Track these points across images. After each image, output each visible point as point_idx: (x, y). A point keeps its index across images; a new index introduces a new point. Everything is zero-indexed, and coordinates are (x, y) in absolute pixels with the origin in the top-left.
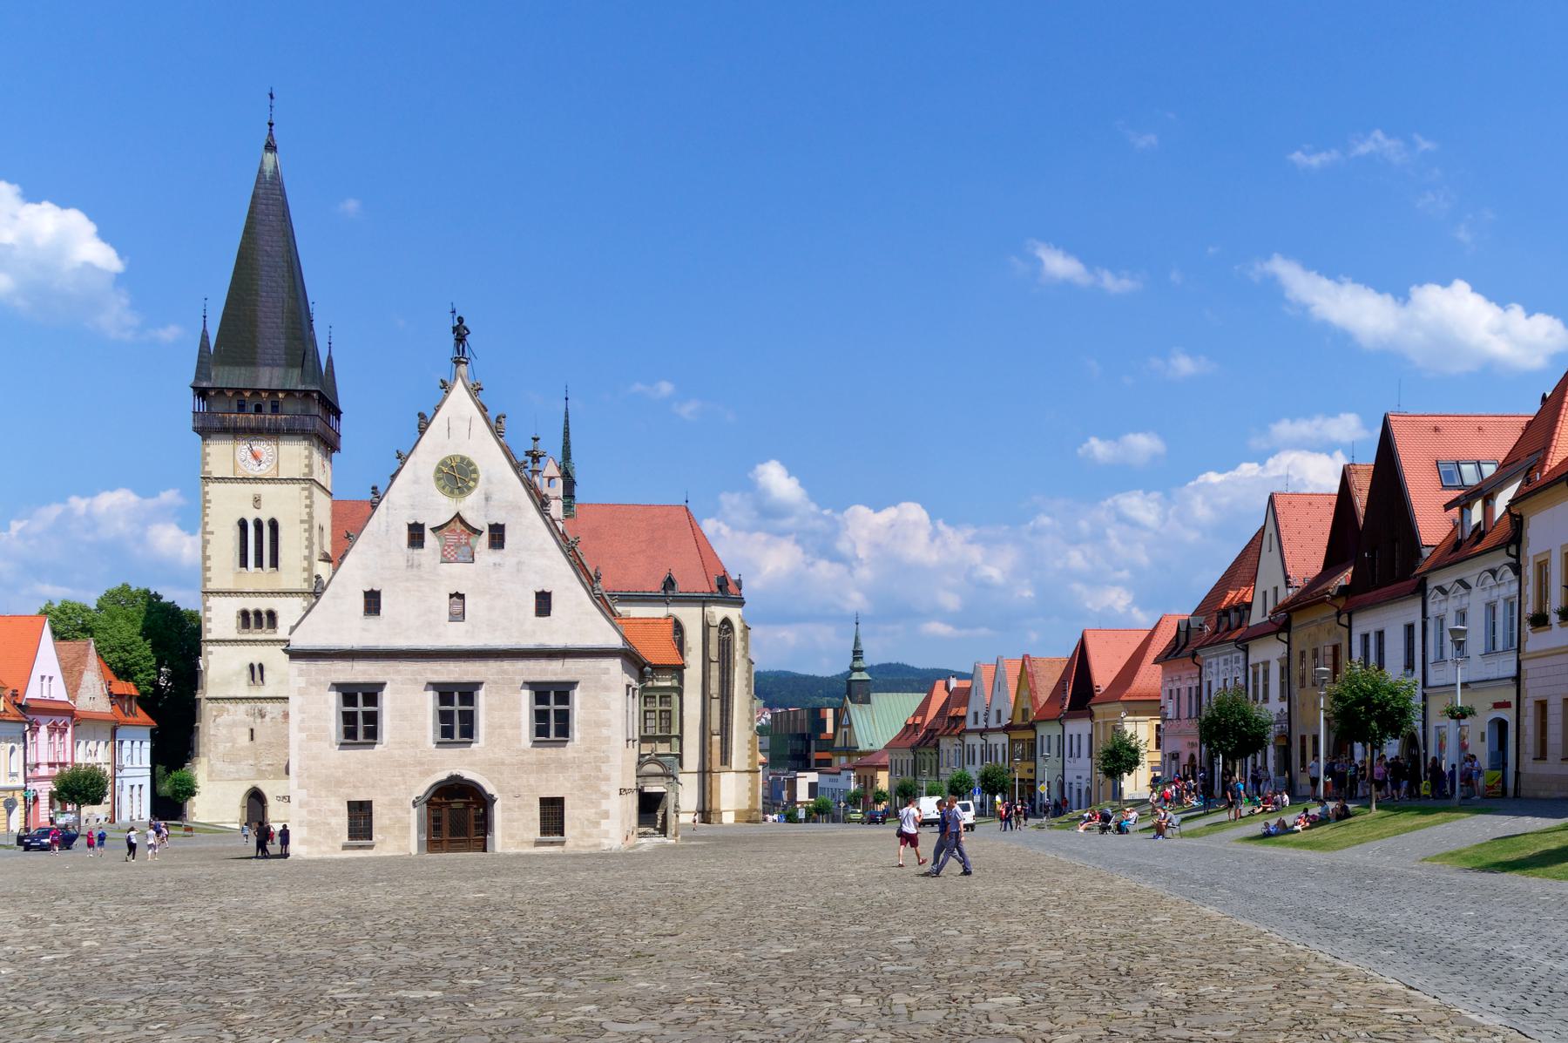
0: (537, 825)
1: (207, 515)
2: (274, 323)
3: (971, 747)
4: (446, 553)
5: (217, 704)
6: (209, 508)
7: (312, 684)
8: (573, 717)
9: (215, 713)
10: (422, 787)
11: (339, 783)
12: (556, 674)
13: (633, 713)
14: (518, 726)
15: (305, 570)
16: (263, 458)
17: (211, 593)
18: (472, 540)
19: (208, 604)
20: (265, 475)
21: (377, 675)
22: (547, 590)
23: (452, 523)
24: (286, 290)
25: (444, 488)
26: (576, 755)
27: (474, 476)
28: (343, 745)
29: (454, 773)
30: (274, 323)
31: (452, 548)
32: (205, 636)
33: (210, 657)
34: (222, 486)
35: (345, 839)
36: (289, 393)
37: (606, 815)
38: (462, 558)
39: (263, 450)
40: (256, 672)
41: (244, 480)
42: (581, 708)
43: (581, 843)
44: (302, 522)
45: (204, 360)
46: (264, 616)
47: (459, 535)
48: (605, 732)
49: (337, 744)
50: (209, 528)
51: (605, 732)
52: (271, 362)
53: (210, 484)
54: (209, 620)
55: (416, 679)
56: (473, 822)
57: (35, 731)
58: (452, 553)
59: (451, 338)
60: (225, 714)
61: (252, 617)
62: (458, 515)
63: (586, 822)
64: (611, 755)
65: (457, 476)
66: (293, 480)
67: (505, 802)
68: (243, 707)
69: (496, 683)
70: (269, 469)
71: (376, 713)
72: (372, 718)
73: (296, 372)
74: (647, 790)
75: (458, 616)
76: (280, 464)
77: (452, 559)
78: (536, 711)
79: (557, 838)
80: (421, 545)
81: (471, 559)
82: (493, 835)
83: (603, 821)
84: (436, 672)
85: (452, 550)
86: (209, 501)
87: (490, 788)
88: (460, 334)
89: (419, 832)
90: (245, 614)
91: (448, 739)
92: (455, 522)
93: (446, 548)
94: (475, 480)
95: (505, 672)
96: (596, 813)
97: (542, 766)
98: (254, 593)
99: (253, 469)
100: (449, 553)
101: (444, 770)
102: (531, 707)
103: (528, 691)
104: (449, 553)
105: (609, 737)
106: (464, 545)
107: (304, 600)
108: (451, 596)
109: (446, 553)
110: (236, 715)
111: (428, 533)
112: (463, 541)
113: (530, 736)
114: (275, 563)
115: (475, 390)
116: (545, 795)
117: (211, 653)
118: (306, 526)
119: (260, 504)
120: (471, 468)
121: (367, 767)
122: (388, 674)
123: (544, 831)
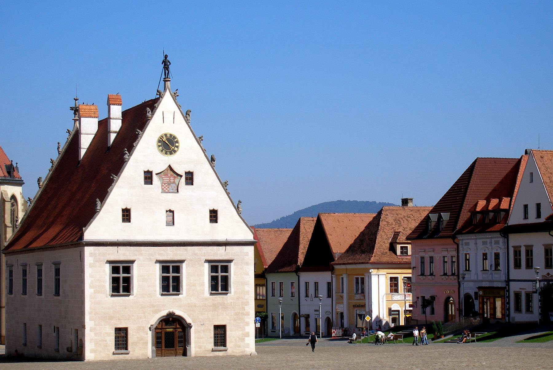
0: (212, 340)
4: (163, 187)
7: (97, 262)
10: (154, 320)
11: (111, 318)
12: (221, 256)
14: (203, 285)
18: (177, 181)
21: (130, 256)
22: (216, 209)
25: (162, 151)
26: (232, 301)
27: (177, 144)
28: (112, 296)
29: (171, 311)
31: (166, 184)
35: (113, 349)
37: (247, 335)
38: (172, 191)
42: (234, 275)
43: (235, 351)
48: (246, 288)
49: (109, 295)
51: (246, 288)
55: (150, 258)
56: (177, 340)
58: (167, 187)
62: (170, 166)
63: (237, 339)
64: (249, 301)
67: (197, 328)
75: (172, 223)
78: (212, 276)
79: (223, 348)
82: (190, 347)
83: (246, 338)
84: (160, 254)
85: (166, 186)
87: (189, 320)
88: (166, 64)
89: (153, 345)
91: (166, 293)
92: (168, 170)
93: (163, 184)
94: (177, 147)
95: (196, 254)
96: (242, 334)
97: (215, 307)
101: (165, 310)
102: (209, 274)
103: (159, 264)
104: (165, 187)
105: (249, 291)
106: (172, 183)
108: (167, 211)
109: (163, 187)
112: (172, 181)
113: (209, 291)
115: (175, 96)
116: (217, 324)
120: (175, 140)
121: (125, 308)
123: (216, 344)
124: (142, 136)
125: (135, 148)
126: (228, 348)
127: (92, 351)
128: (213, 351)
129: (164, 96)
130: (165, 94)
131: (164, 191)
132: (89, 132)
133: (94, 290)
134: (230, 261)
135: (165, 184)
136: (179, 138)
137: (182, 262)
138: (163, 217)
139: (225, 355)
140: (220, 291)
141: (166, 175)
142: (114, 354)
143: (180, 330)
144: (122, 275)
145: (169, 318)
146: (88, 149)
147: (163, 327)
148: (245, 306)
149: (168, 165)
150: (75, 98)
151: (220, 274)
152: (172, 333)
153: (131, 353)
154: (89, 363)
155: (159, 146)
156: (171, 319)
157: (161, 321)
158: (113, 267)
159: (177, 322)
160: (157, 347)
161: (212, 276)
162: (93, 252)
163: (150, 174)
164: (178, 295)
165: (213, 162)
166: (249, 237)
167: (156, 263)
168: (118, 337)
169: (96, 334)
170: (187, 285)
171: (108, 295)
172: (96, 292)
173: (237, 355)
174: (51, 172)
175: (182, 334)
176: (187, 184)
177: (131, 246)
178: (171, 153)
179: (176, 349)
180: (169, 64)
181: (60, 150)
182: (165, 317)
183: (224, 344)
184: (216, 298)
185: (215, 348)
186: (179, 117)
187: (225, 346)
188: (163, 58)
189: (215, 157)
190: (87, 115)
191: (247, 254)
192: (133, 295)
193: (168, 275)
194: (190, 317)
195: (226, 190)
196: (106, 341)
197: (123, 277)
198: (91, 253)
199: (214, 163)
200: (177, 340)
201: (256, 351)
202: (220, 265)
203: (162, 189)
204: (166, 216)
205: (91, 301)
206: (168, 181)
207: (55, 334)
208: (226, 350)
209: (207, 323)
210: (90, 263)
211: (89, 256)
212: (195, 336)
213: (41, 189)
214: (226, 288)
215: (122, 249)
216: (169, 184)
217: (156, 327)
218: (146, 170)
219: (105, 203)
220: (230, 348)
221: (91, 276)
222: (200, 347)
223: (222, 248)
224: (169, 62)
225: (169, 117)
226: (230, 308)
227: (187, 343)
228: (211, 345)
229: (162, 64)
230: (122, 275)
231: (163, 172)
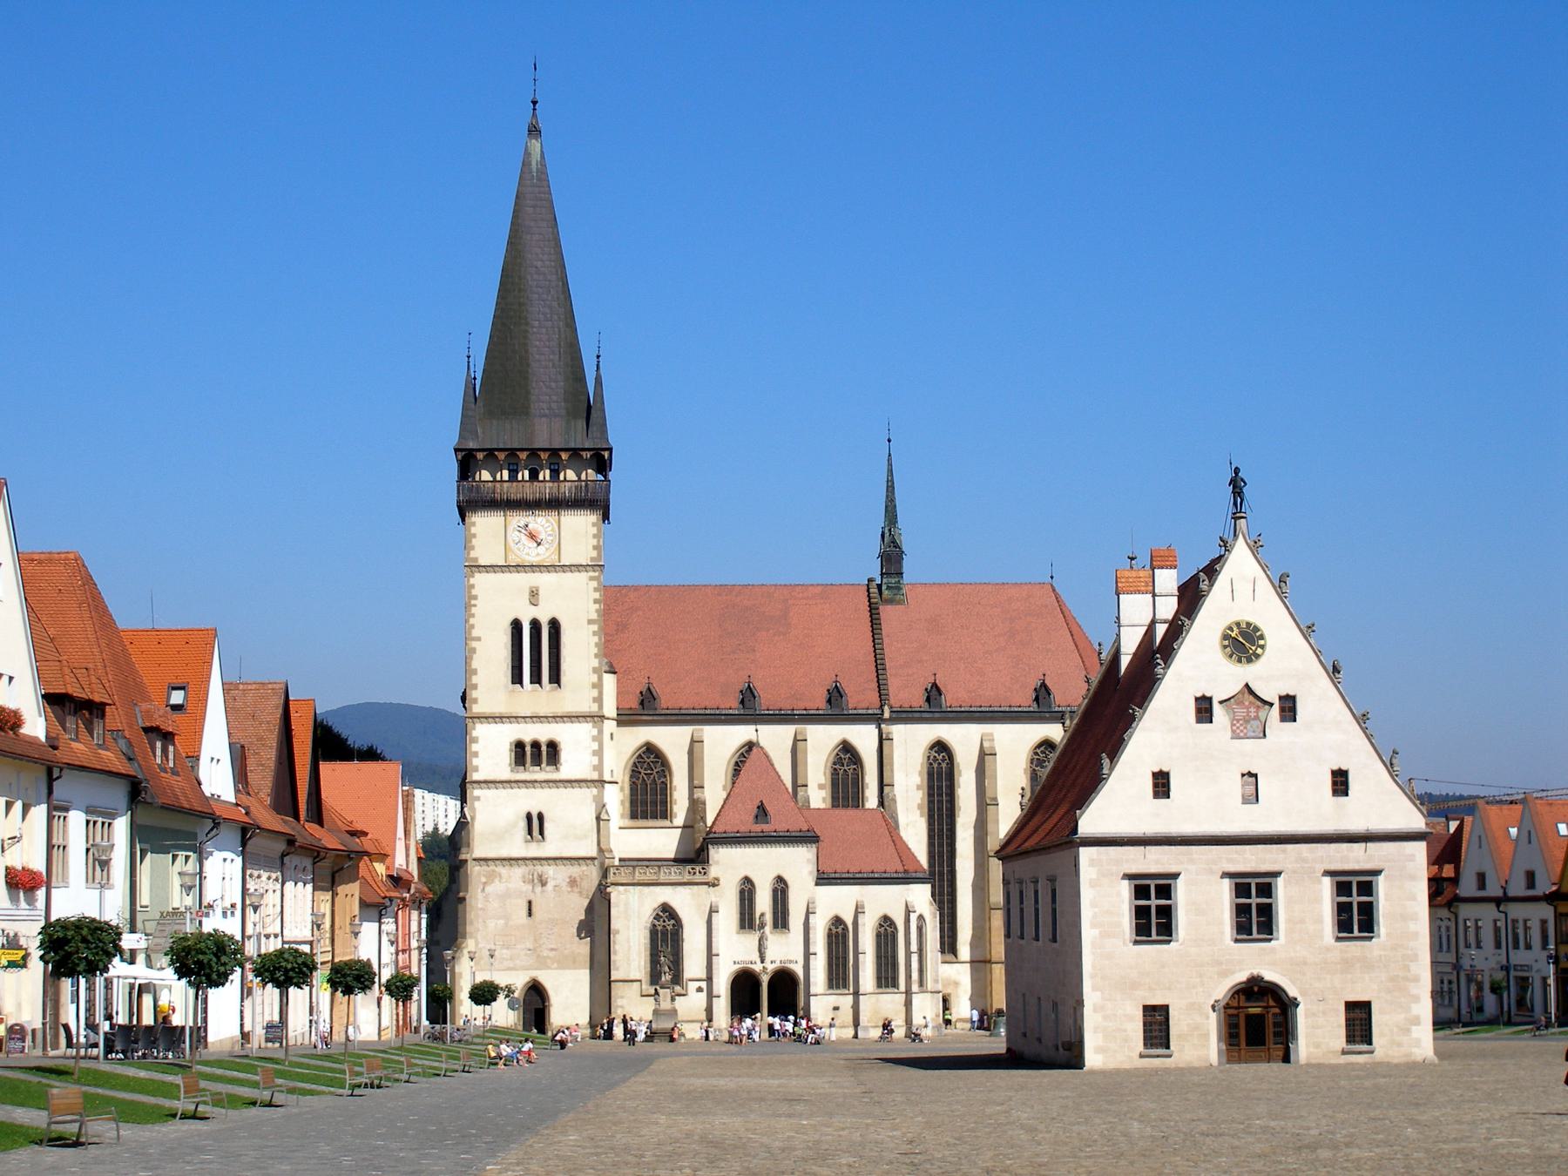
1: (473, 616)
2: (550, 360)
3: (1521, 925)
4: (1234, 728)
5: (485, 868)
6: (475, 606)
8: (1378, 910)
9: (484, 880)
10: (1221, 990)
14: (1320, 921)
15: (594, 686)
16: (542, 536)
17: (478, 718)
18: (1262, 714)
19: (475, 733)
20: (544, 560)
21: (1170, 864)
22: (1344, 768)
23: (1240, 696)
24: (562, 317)
25: (1231, 656)
26: (1382, 953)
27: (1261, 642)
28: (1136, 942)
29: (1255, 972)
30: (550, 360)
31: (1241, 722)
32: (471, 776)
33: (477, 804)
35: (1140, 1046)
36: (575, 453)
37: (1416, 1021)
38: (1253, 734)
39: (541, 529)
40: (535, 824)
41: (520, 568)
42: (1386, 900)
44: (590, 622)
45: (470, 413)
46: (544, 748)
47: (1248, 708)
48: (1412, 927)
49: (1131, 942)
50: (475, 633)
51: (1412, 927)
52: (547, 411)
53: (477, 575)
54: (476, 754)
56: (1272, 1030)
58: (1242, 728)
60: (497, 881)
61: (528, 749)
63: (1395, 1030)
67: (1309, 1007)
68: (518, 872)
69: (1295, 872)
70: (547, 554)
71: (1169, 907)
72: (1166, 913)
76: (562, 546)
77: (1242, 734)
78: (1338, 903)
79: (1365, 1047)
81: (1262, 735)
83: (1414, 1028)
84: (1230, 861)
85: (1241, 725)
86: (475, 598)
87: (1292, 991)
88: (1237, 486)
89: (1219, 1040)
90: (519, 746)
91: (1245, 937)
92: (1243, 694)
93: (1235, 722)
94: (1262, 647)
95: (1304, 860)
97: (1347, 965)
98: (531, 717)
99: (528, 554)
100: (1238, 728)
101: (1244, 970)
102: (1333, 901)
104: (1238, 728)
107: (593, 727)
108: (1243, 775)
109: (1234, 728)
110: (509, 883)
111: (1216, 706)
112: (1253, 715)
113: (1333, 932)
114: (556, 678)
115: (1255, 547)
117: (478, 798)
118: (595, 627)
119: (538, 600)
120: (1258, 634)
122: (1182, 863)
123: (1351, 1038)
124: (1190, 629)
125: (1177, 653)
126: (1375, 1048)
127: (1099, 1050)
128: (1344, 1052)
129: (1232, 549)
130: (1234, 544)
131: (1236, 736)
132: (1136, 622)
133: (1100, 933)
134: (1377, 873)
135: (1238, 721)
136: (1265, 629)
137: (1276, 874)
138: (1236, 787)
139: (1370, 1061)
140: (1356, 933)
141: (1240, 703)
142: (1141, 1056)
143: (1277, 1010)
144: (1154, 902)
145: (1252, 987)
146: (1135, 654)
147: (1241, 1005)
148: (1411, 964)
149: (1244, 683)
150: (1131, 556)
151: (1356, 899)
152: (1260, 1018)
153: (1175, 1055)
154: (1092, 1072)
155: (1225, 647)
156: (1256, 989)
157: (1237, 992)
158: (1136, 886)
159: (1270, 996)
160: (1230, 1045)
161: (1338, 903)
162: (1095, 857)
163: (1208, 702)
164: (1270, 940)
165: (1336, 674)
166: (1417, 822)
167: (1222, 877)
168: (1151, 1024)
169: (1105, 1018)
170: (1289, 921)
171: (1128, 942)
173: (1396, 1061)
174: (1086, 701)
175: (1280, 1019)
176: (1283, 719)
177: (1171, 845)
178: (1249, 661)
179: (1269, 1049)
180: (1243, 484)
181: (1103, 656)
182: (1243, 985)
183: (1368, 1040)
184: (1348, 946)
185: (1349, 1047)
186: (1266, 589)
187: (1370, 1043)
188: (1230, 475)
189: (1342, 665)
190: (1131, 589)
191: (1411, 858)
192: (1177, 941)
194: (1293, 982)
195: (1364, 730)
196: (1125, 1031)
197: (1157, 906)
198: (1093, 860)
199: (1337, 675)
200: (1270, 1030)
201: (1435, 1054)
202: (1354, 880)
203: (1233, 731)
204: (1243, 785)
205: (1093, 954)
206: (1245, 714)
207: (1053, 1016)
208: (1372, 1052)
209: (1331, 997)
210: (1091, 879)
211: (1089, 866)
212: (1306, 1023)
213: (1068, 734)
214: (1368, 925)
215: (1153, 851)
216: (1247, 722)
217: (1227, 1004)
218: (1199, 695)
219: (1118, 761)
220: (1381, 1047)
221: (1093, 905)
222: (1317, 1046)
223: (1358, 847)
224: (1242, 480)
225: (1244, 589)
226: (1379, 967)
227: (1290, 1037)
228: (1338, 1038)
229: (1230, 485)
230: (1154, 902)
231: (1236, 698)
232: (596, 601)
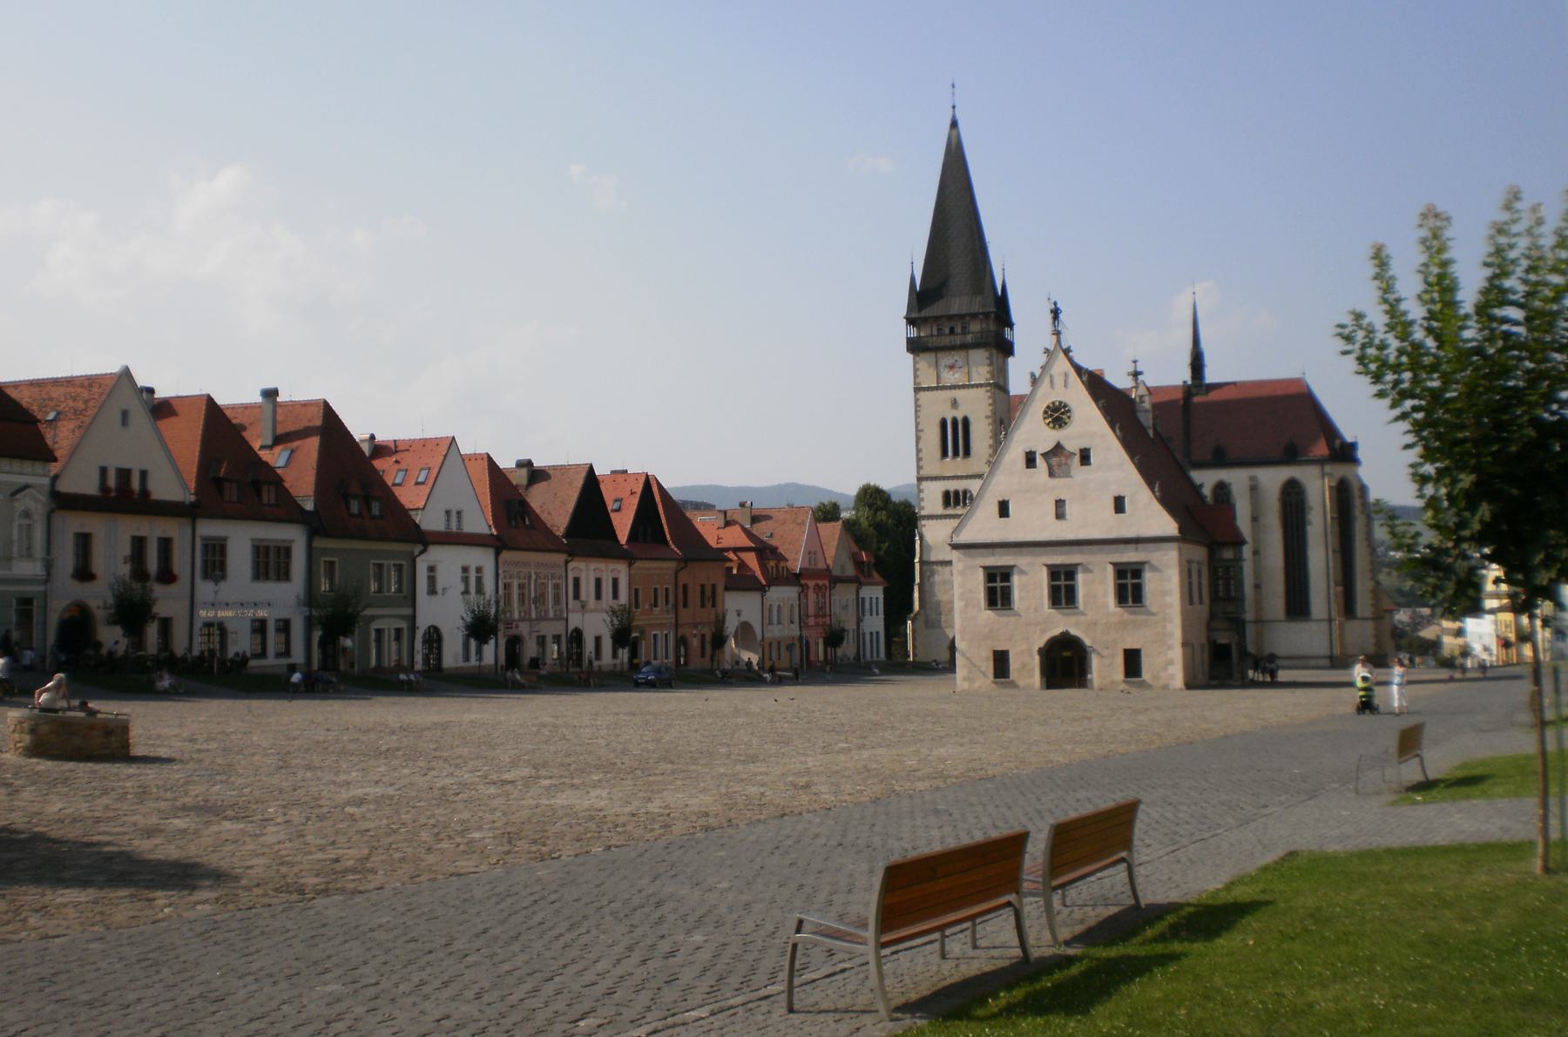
10: (1041, 642)
13: (1200, 584)
33: (924, 529)
34: (927, 393)
37: (1171, 662)
48: (1168, 599)
50: (920, 428)
51: (1168, 599)
57: (804, 588)
59: (1050, 316)
65: (1058, 415)
66: (977, 386)
73: (978, 299)
74: (1222, 641)
75: (1060, 515)
80: (1034, 466)
87: (1087, 642)
88: (1056, 313)
90: (946, 495)
97: (1123, 625)
102: (1115, 583)
114: (967, 453)
117: (924, 526)
118: (990, 420)
131: (1051, 474)
136: (1072, 404)
138: (1051, 509)
172: (966, 606)
193: (1134, 581)
225: (1059, 381)
230: (998, 584)
232: (990, 405)
